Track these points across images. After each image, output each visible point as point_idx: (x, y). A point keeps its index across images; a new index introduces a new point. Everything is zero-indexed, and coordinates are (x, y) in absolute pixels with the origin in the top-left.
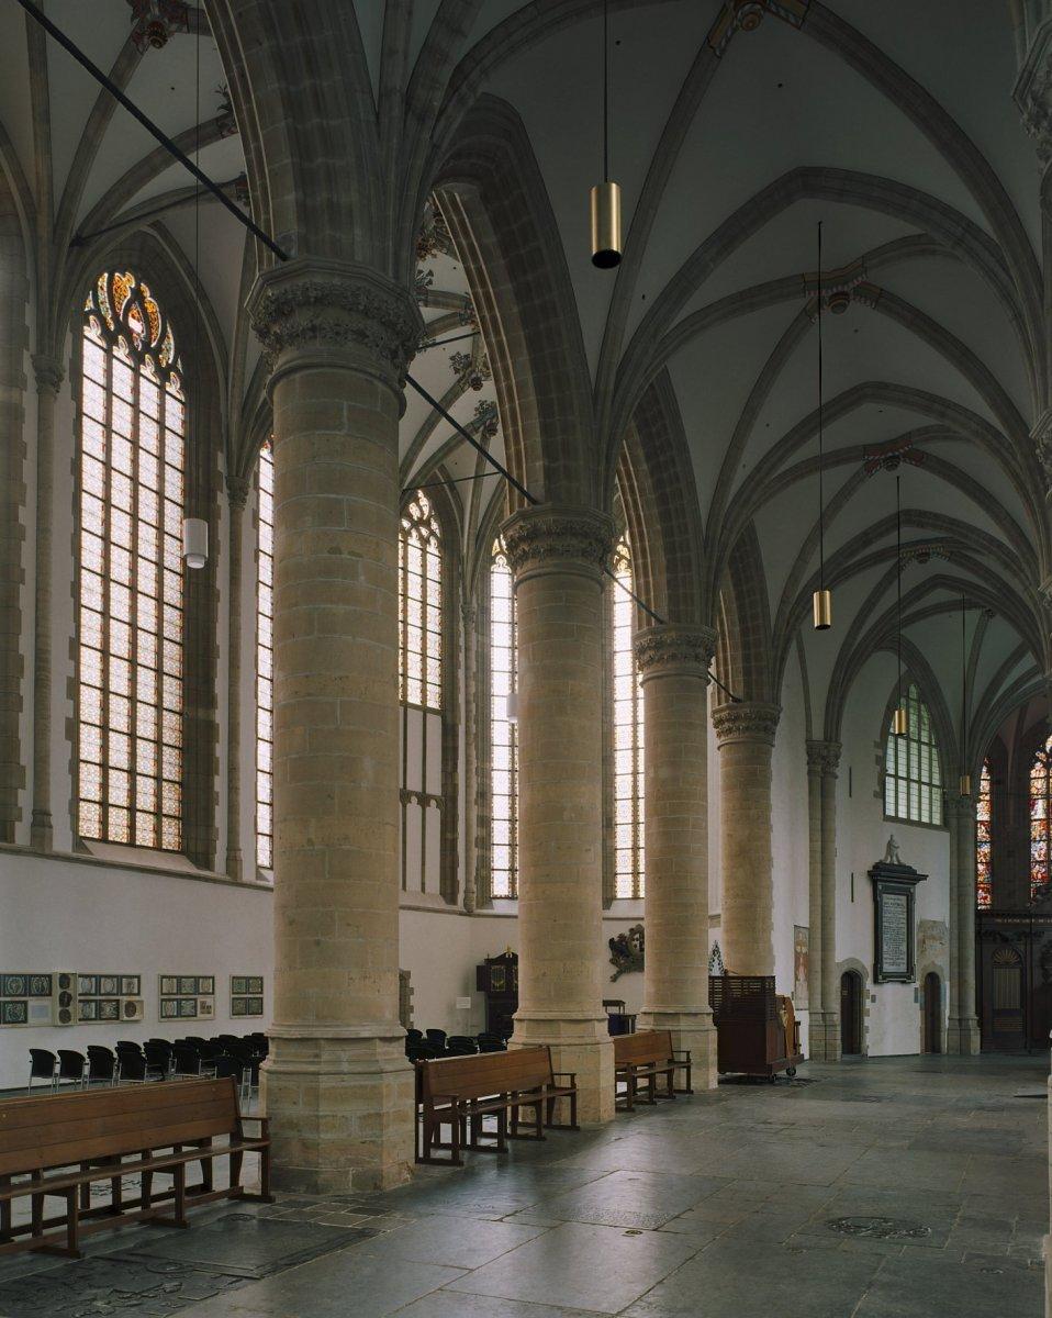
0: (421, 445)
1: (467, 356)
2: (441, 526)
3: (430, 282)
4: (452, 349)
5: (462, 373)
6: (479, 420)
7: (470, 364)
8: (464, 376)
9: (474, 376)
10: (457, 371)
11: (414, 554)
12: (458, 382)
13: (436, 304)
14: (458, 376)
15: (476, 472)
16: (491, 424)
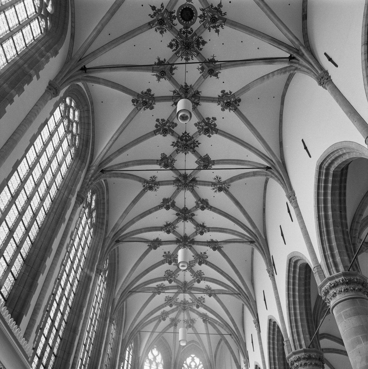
0: (138, 317)
1: (170, 297)
2: (134, 345)
3: (177, 277)
4: (167, 295)
5: (167, 301)
6: (161, 315)
7: (171, 300)
8: (167, 302)
9: (171, 303)
10: (166, 300)
11: (127, 353)
12: (165, 303)
13: (176, 282)
14: (165, 302)
15: (153, 330)
16: (164, 318)
